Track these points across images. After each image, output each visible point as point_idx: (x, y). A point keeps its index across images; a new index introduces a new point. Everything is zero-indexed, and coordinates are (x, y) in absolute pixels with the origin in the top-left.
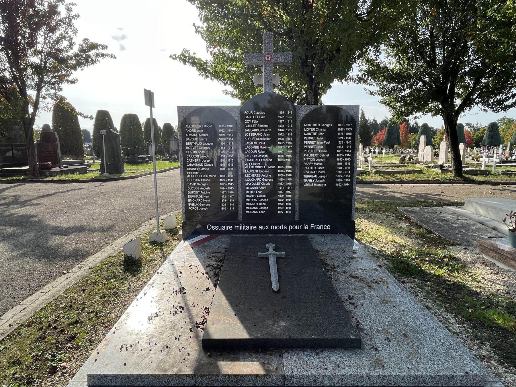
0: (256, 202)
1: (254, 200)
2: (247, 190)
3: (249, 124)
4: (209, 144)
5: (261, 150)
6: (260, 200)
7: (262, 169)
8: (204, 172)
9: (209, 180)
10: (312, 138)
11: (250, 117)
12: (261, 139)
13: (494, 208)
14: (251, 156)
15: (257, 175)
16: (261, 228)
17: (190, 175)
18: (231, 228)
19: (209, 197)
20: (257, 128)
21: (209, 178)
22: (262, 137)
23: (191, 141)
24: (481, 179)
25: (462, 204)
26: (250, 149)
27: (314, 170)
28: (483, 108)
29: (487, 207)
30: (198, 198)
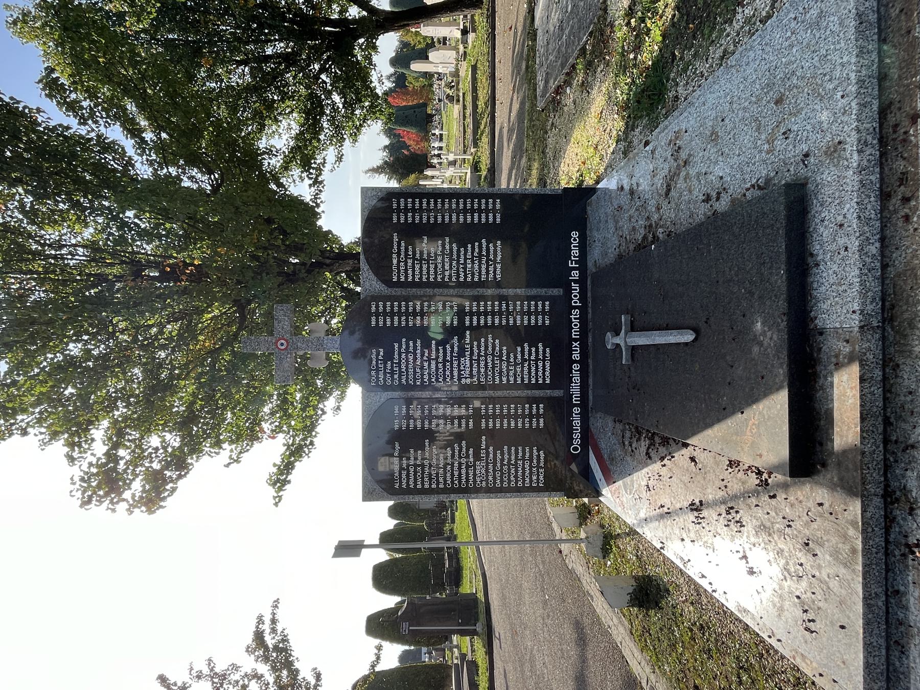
1: (526, 369)
2: (508, 380)
3: (392, 377)
5: (437, 357)
6: (526, 357)
7: (472, 354)
9: (491, 448)
10: (417, 267)
11: (381, 376)
12: (419, 355)
14: (448, 373)
15: (482, 364)
16: (576, 356)
17: (481, 481)
18: (576, 410)
19: (520, 449)
20: (399, 364)
21: (487, 448)
22: (415, 354)
23: (423, 478)
26: (437, 374)
27: (473, 263)
30: (523, 469)
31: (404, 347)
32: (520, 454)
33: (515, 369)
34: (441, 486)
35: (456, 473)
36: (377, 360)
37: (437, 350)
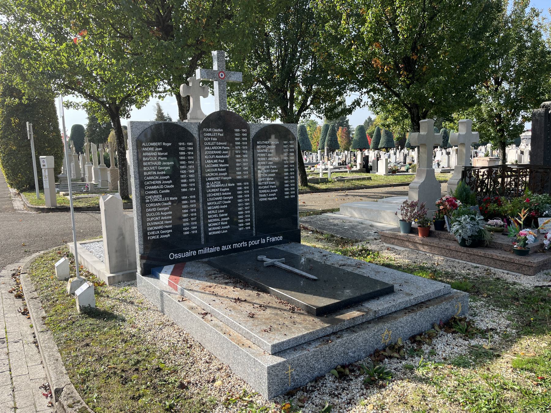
0: (218, 222)
1: (215, 220)
2: (209, 210)
3: (209, 141)
4: (168, 163)
5: (220, 168)
7: (223, 188)
8: (164, 195)
10: (264, 155)
11: (209, 134)
12: (220, 157)
13: (366, 209)
14: (212, 174)
15: (218, 194)
16: (224, 248)
17: (149, 199)
18: (194, 253)
19: (171, 222)
20: (216, 145)
22: (221, 154)
23: (149, 161)
24: (323, 186)
25: (338, 210)
27: (267, 185)
28: (318, 115)
29: (360, 210)
30: (158, 225)
31: (225, 148)
32: (167, 222)
33: (216, 214)
34: (145, 173)
35: (154, 183)
36: (218, 132)
37: (223, 168)
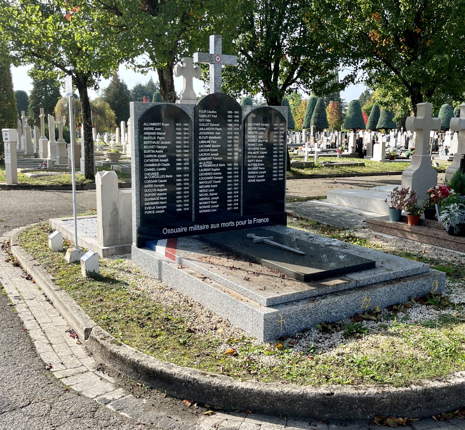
0: (208, 200)
2: (201, 189)
3: (203, 122)
4: (166, 143)
6: (212, 198)
7: (214, 168)
8: (161, 173)
9: (166, 181)
12: (213, 138)
13: (356, 197)
15: (209, 174)
16: (213, 226)
17: (148, 176)
18: (185, 229)
21: (166, 179)
22: (214, 135)
24: (308, 172)
25: (325, 197)
26: (204, 148)
28: (305, 90)
29: (349, 197)
31: (218, 129)
32: (163, 198)
33: (206, 192)
34: (145, 152)
35: (152, 160)
36: (212, 114)
